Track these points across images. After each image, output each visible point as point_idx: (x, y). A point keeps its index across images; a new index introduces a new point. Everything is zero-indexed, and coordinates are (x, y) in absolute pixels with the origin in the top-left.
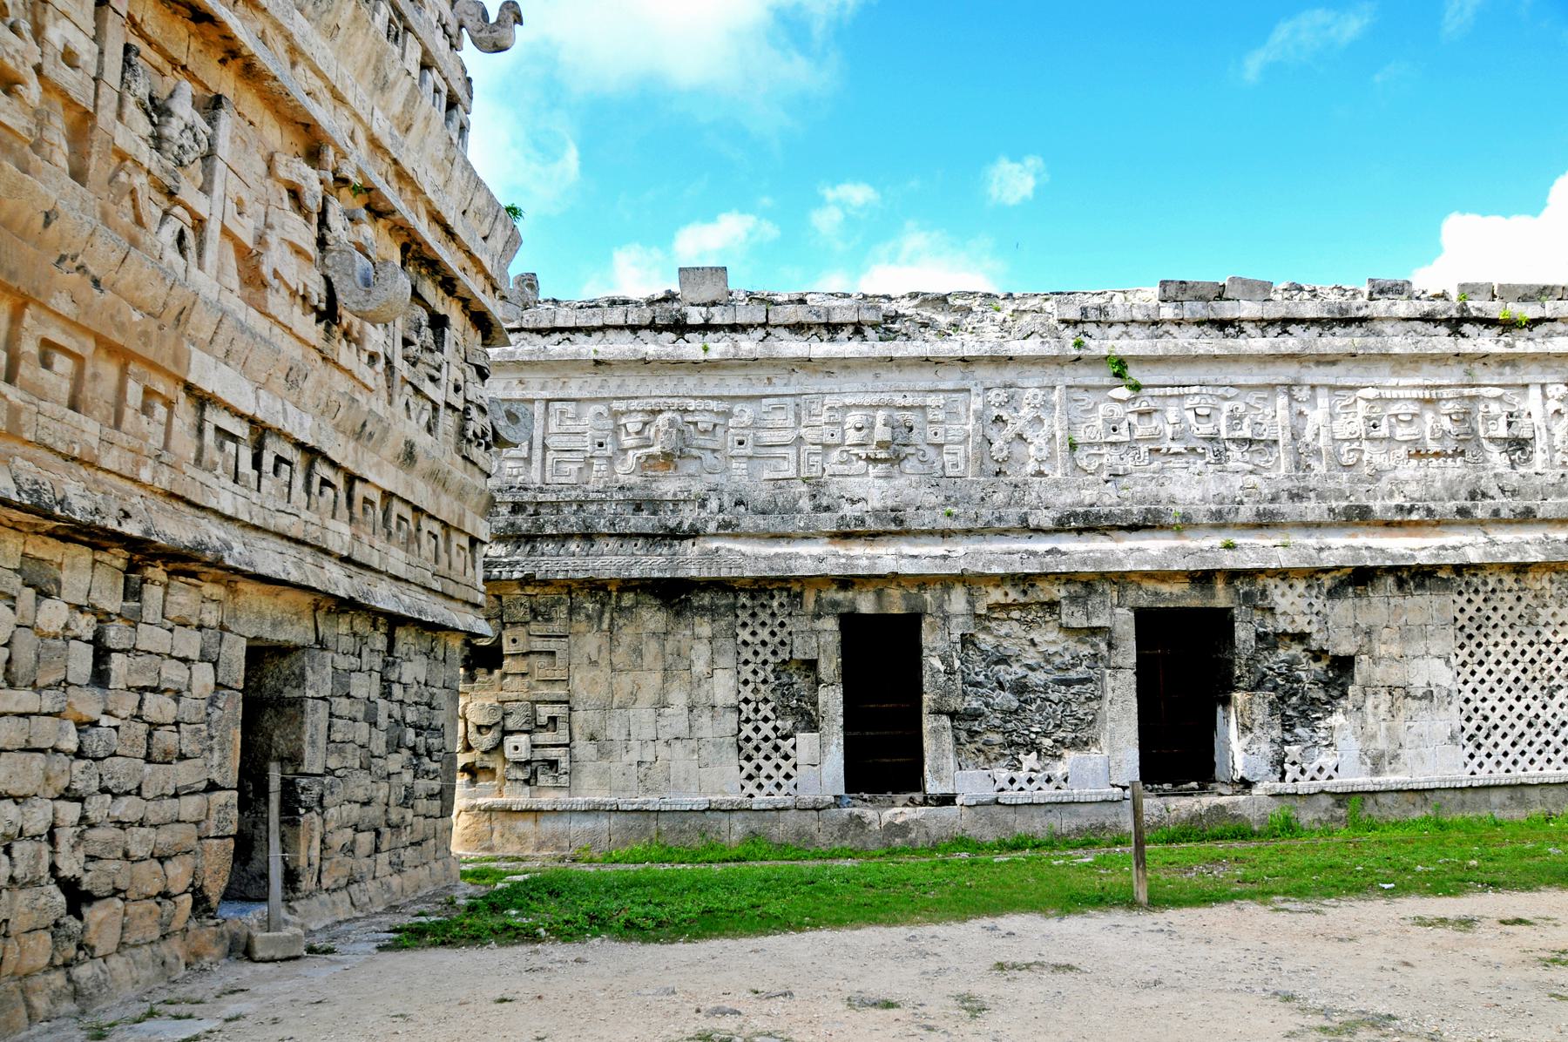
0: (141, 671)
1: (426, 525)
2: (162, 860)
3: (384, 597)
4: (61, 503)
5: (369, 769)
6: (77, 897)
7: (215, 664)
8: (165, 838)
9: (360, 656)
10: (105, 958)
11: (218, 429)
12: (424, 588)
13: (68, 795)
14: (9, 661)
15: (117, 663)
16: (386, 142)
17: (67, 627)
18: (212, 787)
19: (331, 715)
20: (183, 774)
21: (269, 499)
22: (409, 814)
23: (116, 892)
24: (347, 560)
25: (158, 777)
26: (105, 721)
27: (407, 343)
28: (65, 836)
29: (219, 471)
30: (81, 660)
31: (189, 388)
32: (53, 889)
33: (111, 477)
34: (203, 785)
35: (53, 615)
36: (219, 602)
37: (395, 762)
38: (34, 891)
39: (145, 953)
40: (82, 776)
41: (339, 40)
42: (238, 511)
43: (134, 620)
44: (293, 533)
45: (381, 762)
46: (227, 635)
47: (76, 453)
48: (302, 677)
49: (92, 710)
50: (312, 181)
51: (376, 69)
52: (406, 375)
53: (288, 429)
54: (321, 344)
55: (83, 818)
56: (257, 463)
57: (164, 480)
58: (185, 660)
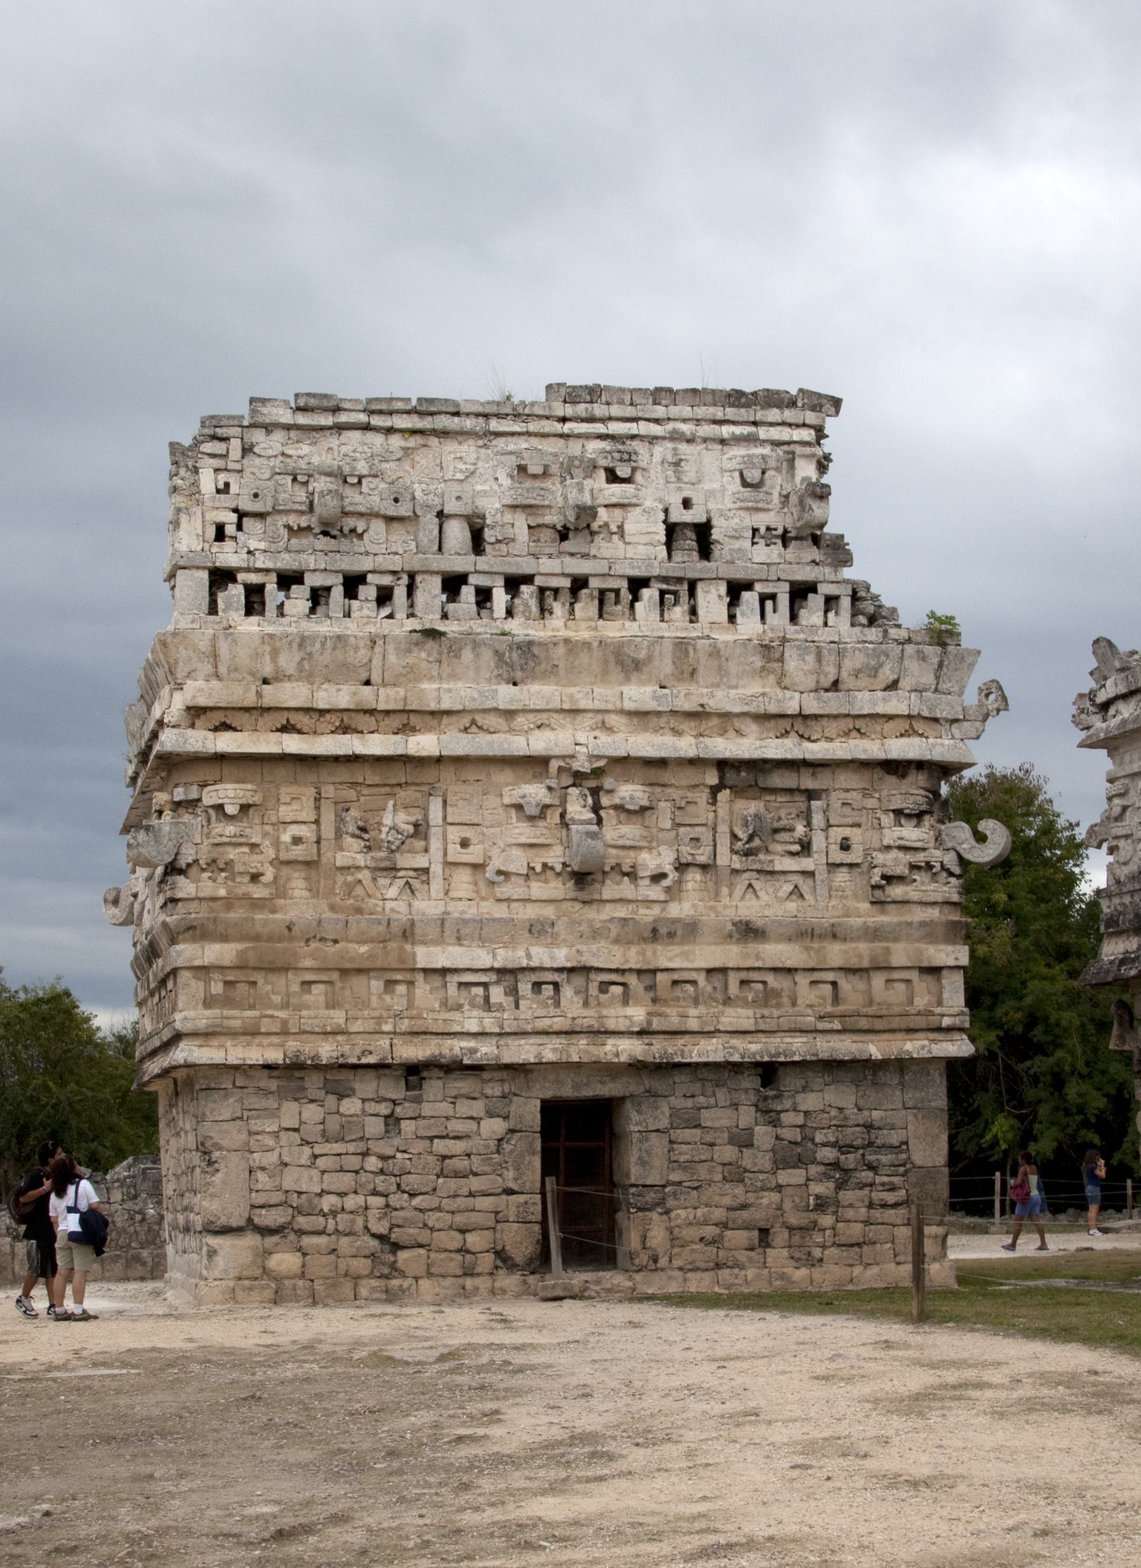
0: (429, 1127)
1: (803, 980)
2: (463, 1231)
3: (710, 1050)
4: (312, 1059)
5: (742, 1181)
6: (396, 1247)
7: (506, 1118)
8: (459, 1219)
9: (714, 1094)
10: (417, 1279)
11: (460, 984)
12: (802, 1031)
13: (375, 1193)
14: (324, 1131)
15: (407, 1126)
16: (652, 705)
17: (363, 1111)
18: (509, 1192)
19: (671, 1142)
20: (475, 1184)
21: (532, 1010)
22: (827, 1220)
23: (421, 1246)
24: (641, 1033)
25: (447, 1185)
26: (399, 1155)
27: (734, 837)
28: (373, 1214)
29: (466, 1007)
30: (375, 1127)
31: (426, 971)
32: (367, 1238)
33: (360, 1037)
34: (499, 1190)
35: (351, 1106)
36: (502, 1081)
37: (783, 1177)
38: (351, 1238)
39: (448, 1282)
40: (380, 1182)
41: (562, 672)
42: (473, 1030)
43: (418, 1100)
44: (556, 1028)
45: (761, 1177)
46: (515, 1099)
47: (329, 1029)
48: (629, 1118)
49: (389, 1151)
50: (535, 792)
51: (620, 662)
52: (737, 866)
53: (533, 964)
54: (571, 895)
55: (387, 1206)
56: (513, 992)
57: (404, 1025)
58: (472, 1118)
